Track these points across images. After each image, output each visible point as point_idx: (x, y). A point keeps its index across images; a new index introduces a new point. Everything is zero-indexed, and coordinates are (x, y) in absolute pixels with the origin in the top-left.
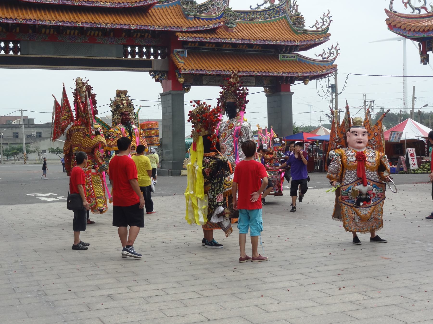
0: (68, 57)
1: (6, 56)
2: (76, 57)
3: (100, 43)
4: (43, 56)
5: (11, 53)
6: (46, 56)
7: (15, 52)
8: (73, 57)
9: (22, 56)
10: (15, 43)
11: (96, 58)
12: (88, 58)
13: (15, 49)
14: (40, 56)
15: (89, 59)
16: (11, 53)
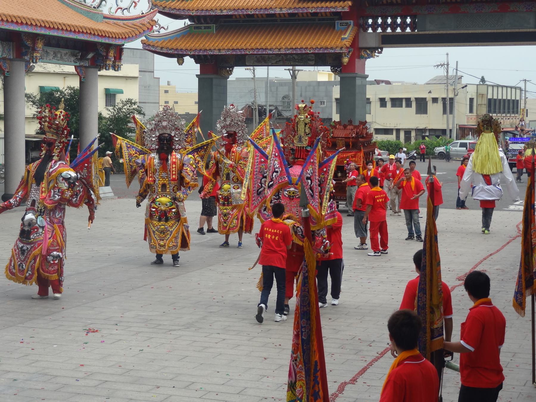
0: (470, 32)
1: (393, 35)
2: (480, 31)
3: (513, 11)
4: (441, 32)
5: (408, 30)
6: (444, 32)
7: (413, 29)
8: (477, 31)
9: (420, 33)
10: (413, 17)
11: (506, 31)
12: (495, 31)
13: (413, 26)
14: (436, 32)
15: (497, 33)
16: (408, 30)
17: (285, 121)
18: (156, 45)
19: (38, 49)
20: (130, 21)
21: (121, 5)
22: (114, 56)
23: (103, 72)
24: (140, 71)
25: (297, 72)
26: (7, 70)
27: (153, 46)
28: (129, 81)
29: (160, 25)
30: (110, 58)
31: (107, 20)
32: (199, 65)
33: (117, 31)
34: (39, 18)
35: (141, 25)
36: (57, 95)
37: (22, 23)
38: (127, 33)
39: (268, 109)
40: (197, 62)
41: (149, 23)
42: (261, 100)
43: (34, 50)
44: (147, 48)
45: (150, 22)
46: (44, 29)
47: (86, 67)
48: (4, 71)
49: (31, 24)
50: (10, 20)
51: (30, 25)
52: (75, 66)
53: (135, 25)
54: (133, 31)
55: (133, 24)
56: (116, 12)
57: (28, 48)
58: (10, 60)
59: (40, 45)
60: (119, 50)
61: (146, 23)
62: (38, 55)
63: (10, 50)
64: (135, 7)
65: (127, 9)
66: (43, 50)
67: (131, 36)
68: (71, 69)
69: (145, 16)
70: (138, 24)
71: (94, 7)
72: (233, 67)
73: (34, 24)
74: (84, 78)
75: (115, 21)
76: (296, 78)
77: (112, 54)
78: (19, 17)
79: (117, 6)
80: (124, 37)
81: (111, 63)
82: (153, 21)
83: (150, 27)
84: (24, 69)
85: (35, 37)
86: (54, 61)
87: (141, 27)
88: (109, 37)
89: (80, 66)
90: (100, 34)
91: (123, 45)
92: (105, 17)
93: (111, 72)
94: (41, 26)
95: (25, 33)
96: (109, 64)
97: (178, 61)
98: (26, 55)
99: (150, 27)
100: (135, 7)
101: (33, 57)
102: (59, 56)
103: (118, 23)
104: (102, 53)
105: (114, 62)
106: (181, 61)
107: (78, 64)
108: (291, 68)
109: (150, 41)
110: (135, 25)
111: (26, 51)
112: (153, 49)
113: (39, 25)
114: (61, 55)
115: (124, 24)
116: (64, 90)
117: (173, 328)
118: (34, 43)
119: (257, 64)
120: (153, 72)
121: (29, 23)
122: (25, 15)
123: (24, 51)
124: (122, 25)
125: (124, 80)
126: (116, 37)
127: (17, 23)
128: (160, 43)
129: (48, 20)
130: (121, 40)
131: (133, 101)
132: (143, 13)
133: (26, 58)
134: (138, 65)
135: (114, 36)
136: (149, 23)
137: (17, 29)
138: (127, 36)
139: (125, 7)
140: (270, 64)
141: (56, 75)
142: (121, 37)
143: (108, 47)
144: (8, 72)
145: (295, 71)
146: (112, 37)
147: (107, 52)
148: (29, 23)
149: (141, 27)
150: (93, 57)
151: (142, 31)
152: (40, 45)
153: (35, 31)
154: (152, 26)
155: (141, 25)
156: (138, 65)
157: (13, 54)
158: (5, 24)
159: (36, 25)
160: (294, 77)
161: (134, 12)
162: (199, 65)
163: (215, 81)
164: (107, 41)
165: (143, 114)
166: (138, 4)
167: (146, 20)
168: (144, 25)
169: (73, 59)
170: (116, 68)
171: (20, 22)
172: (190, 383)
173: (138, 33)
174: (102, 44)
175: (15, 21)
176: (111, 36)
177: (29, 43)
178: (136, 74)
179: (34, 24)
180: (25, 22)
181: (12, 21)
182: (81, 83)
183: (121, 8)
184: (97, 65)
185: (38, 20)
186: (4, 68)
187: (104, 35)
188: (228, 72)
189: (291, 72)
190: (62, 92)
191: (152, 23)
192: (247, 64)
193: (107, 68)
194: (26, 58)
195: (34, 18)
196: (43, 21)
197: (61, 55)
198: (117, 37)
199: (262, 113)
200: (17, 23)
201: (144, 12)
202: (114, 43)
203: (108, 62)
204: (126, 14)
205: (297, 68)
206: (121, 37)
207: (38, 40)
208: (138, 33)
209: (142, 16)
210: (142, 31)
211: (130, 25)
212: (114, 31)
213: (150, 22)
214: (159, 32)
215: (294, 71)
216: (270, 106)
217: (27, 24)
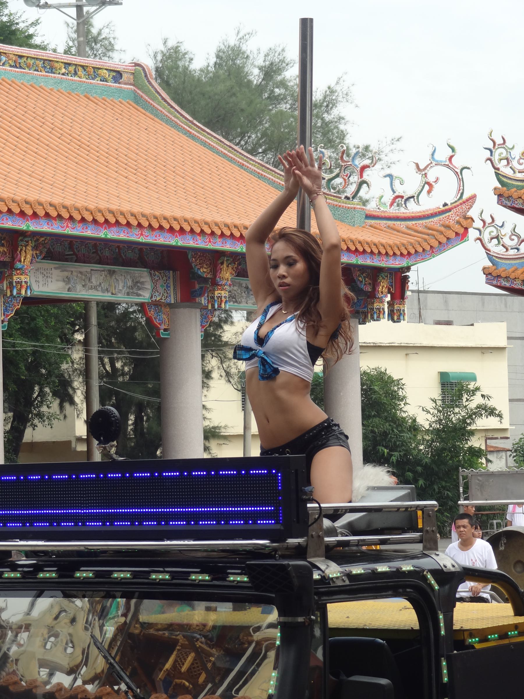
18: (512, 277)
19: (224, 282)
20: (421, 222)
21: (400, 190)
24: (509, 338)
26: (163, 327)
27: (507, 278)
28: (488, 356)
29: (519, 237)
30: (380, 295)
31: (373, 222)
33: (391, 242)
34: (218, 219)
35: (442, 229)
37: (182, 231)
38: (411, 244)
41: (458, 222)
43: (215, 284)
44: (495, 282)
45: (462, 220)
46: (229, 241)
48: (158, 329)
49: (202, 231)
50: (156, 225)
51: (199, 234)
53: (430, 229)
54: (426, 240)
55: (426, 227)
56: (392, 205)
57: (205, 280)
58: (170, 305)
59: (227, 274)
60: (399, 281)
61: (452, 223)
62: (224, 294)
63: (168, 287)
64: (429, 192)
65: (413, 197)
66: (233, 284)
67: (420, 250)
69: (450, 210)
70: (438, 227)
71: (347, 198)
73: (208, 231)
75: (390, 223)
77: (383, 286)
78: (175, 219)
79: (394, 192)
80: (405, 252)
82: (466, 218)
83: (461, 231)
84: (199, 324)
85: (216, 257)
87: (441, 233)
88: (372, 252)
90: (353, 248)
91: (408, 269)
92: (369, 216)
94: (222, 235)
95: (196, 251)
96: (379, 309)
98: (201, 295)
99: (461, 231)
100: (429, 192)
101: (213, 298)
103: (396, 227)
104: (362, 286)
109: (502, 270)
110: (430, 229)
111: (201, 288)
112: (508, 285)
113: (219, 233)
115: (408, 228)
118: (215, 270)
121: (198, 230)
122: (188, 215)
123: (197, 286)
124: (404, 229)
125: (478, 354)
126: (387, 254)
127: (171, 230)
128: (520, 271)
129: (237, 222)
130: (399, 258)
132: (445, 205)
134: (504, 325)
135: (383, 252)
136: (458, 222)
137: (180, 243)
138: (412, 251)
139: (409, 194)
142: (398, 253)
143: (375, 273)
144: (165, 330)
146: (379, 253)
147: (375, 284)
148: (198, 230)
149: (441, 233)
151: (444, 240)
152: (227, 274)
153: (210, 246)
154: (466, 229)
155: (442, 229)
156: (504, 325)
157: (175, 294)
158: (146, 232)
159: (213, 233)
161: (428, 203)
164: (368, 261)
166: (436, 187)
167: (452, 218)
168: (448, 227)
170: (395, 316)
171: (177, 227)
173: (435, 244)
174: (363, 269)
175: (167, 226)
176: (376, 251)
177: (204, 271)
178: (503, 342)
179: (208, 231)
180: (187, 228)
181: (161, 228)
183: (402, 197)
185: (217, 224)
186: (156, 322)
187: (361, 249)
191: (465, 223)
193: (376, 316)
194: (203, 301)
195: (209, 219)
196: (227, 226)
198: (391, 253)
200: (171, 230)
201: (449, 203)
202: (383, 264)
203: (376, 305)
204: (413, 208)
206: (398, 253)
207: (222, 263)
208: (435, 244)
209: (446, 210)
210: (444, 240)
211: (420, 229)
212: (384, 241)
213: (462, 220)
214: (518, 249)
217: (192, 231)
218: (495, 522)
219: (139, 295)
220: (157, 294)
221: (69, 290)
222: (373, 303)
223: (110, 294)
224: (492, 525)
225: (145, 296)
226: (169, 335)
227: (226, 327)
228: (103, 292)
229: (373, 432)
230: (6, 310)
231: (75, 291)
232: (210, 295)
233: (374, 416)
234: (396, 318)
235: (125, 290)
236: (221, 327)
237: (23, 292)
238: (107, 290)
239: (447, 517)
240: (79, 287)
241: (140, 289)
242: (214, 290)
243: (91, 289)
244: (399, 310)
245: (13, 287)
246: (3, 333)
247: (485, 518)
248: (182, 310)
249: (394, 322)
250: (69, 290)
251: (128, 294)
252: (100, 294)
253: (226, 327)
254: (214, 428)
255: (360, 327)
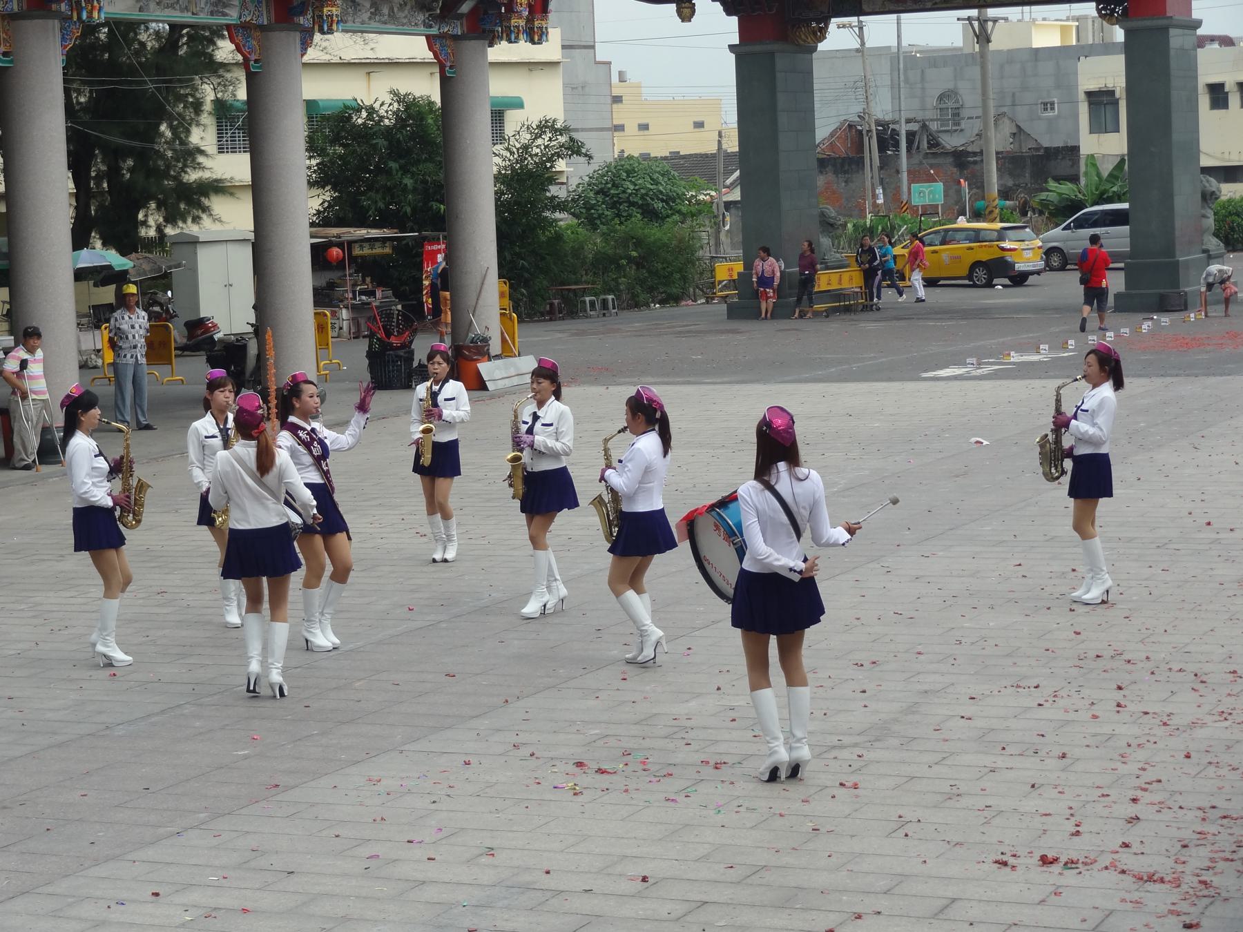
17: (950, 160)
22: (530, 6)
23: (500, 52)
24: (564, 47)
25: (990, 24)
26: (253, 57)
28: (537, 73)
32: (735, 19)
36: (360, 121)
39: (903, 129)
40: (729, 11)
42: (882, 108)
47: (455, 38)
52: (428, 37)
58: (262, 28)
62: (335, 11)
68: (415, 47)
72: (826, 21)
74: (451, 67)
76: (989, 41)
81: (522, 23)
86: (374, 25)
89: (442, 36)
93: (522, 50)
96: (517, 27)
97: (680, 13)
101: (321, 17)
102: (385, 11)
105: (530, 20)
106: (687, 11)
107: (434, 31)
108: (974, 13)
114: (392, 9)
116: (377, 106)
117: (847, 740)
119: (892, 8)
120: (593, 47)
125: (524, 71)
131: (558, 126)
133: (302, 20)
140: (929, 5)
141: (369, 67)
144: (256, 61)
145: (986, 21)
150: (473, 11)
157: (268, 12)
160: (983, 37)
162: (735, 19)
163: (781, 62)
165: (586, 155)
169: (421, 17)
170: (535, 35)
172: (945, 902)
182: (446, 83)
184: (484, 31)
188: (815, 34)
189: (976, 24)
190: (371, 110)
192: (865, 7)
197: (392, 9)
199: (887, 140)
203: (514, 22)
205: (992, 12)
215: (983, 22)
216: (908, 121)
218: (587, 299)
219: (225, 15)
220: (246, 12)
221: (141, 10)
222: (510, 19)
223: (190, 14)
224: (584, 302)
225: (233, 16)
226: (260, 67)
227: (220, 43)
228: (182, 11)
229: (424, 182)
230: (63, 39)
231: (148, 10)
232: (317, 13)
233: (426, 160)
234: (536, 38)
235: (208, 8)
236: (214, 44)
237: (95, 14)
238: (187, 9)
239: (523, 295)
240: (152, 5)
241: (225, 6)
242: (323, 7)
243: (168, 7)
244: (541, 28)
245: (82, 9)
246: (64, 68)
247: (571, 295)
248: (276, 34)
249: (533, 42)
250: (141, 10)
251: (212, 13)
252: (179, 14)
253: (220, 43)
254: (217, 181)
255: (489, 49)
